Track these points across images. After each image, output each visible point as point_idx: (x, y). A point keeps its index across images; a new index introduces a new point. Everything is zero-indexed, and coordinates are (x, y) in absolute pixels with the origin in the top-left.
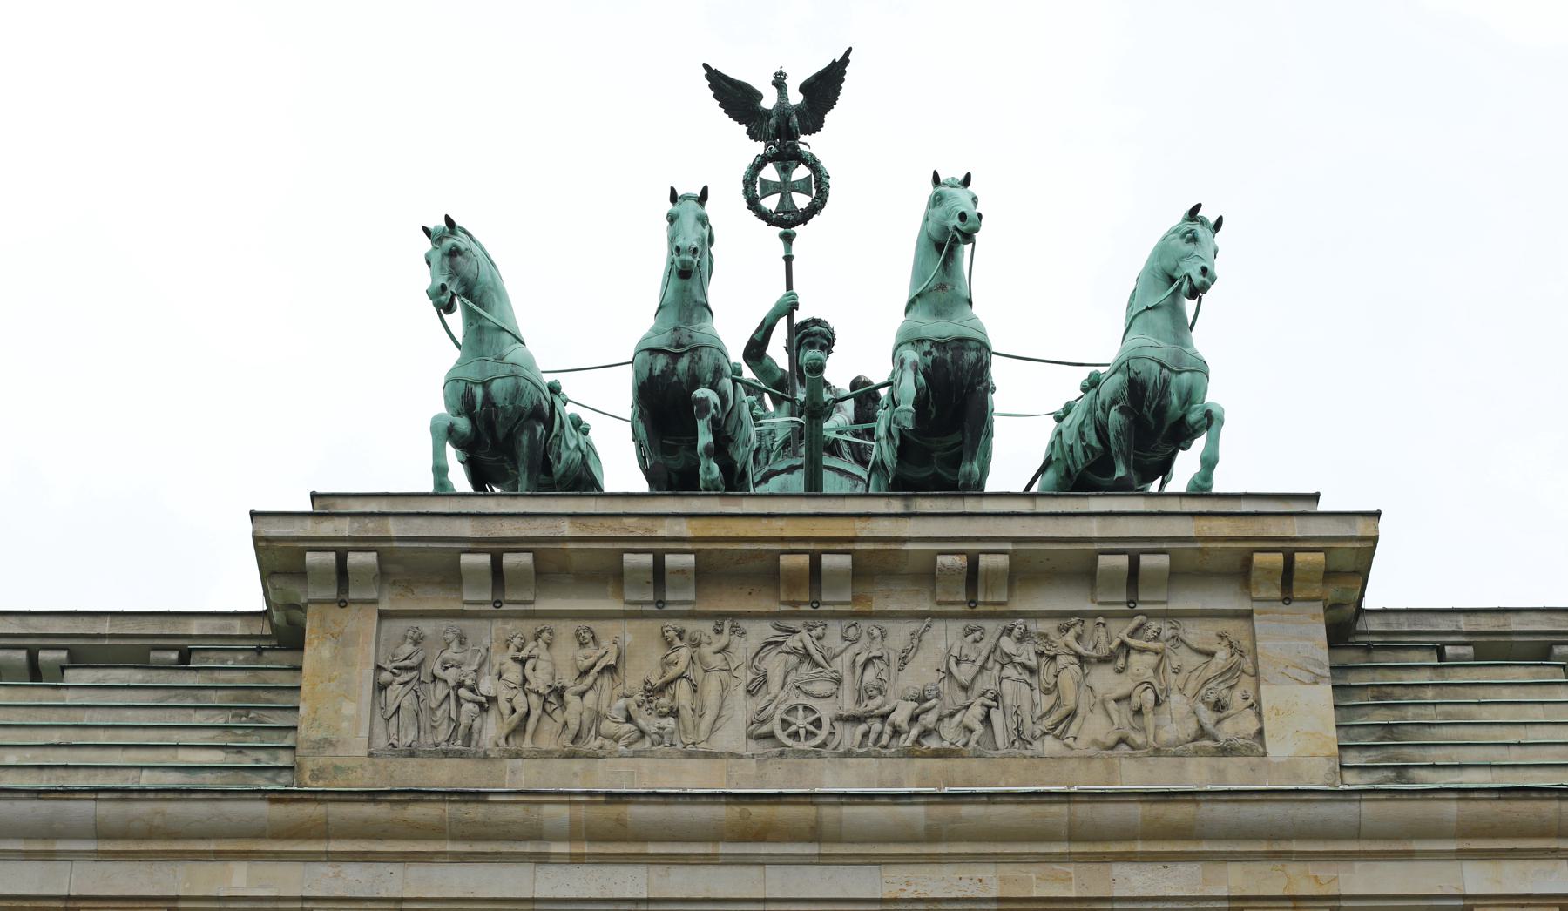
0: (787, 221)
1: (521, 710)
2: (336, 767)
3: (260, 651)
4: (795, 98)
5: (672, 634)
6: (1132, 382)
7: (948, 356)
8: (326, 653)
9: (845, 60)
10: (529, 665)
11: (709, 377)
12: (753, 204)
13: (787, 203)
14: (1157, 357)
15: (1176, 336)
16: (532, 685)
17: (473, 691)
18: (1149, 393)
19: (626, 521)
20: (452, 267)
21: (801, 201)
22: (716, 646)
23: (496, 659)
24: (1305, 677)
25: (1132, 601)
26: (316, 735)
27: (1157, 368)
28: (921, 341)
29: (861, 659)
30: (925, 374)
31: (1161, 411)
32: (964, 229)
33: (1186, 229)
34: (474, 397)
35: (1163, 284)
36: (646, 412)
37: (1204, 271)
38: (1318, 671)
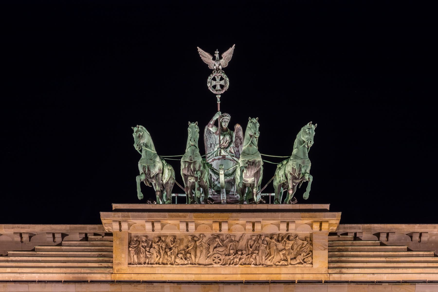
1: (159, 257)
2: (121, 269)
3: (103, 237)
5: (190, 239)
8: (118, 243)
10: (160, 245)
11: (198, 168)
16: (161, 251)
17: (149, 252)
22: (200, 241)
23: (153, 244)
24: (323, 249)
25: (288, 230)
26: (117, 262)
29: (229, 244)
34: (145, 169)
38: (326, 247)
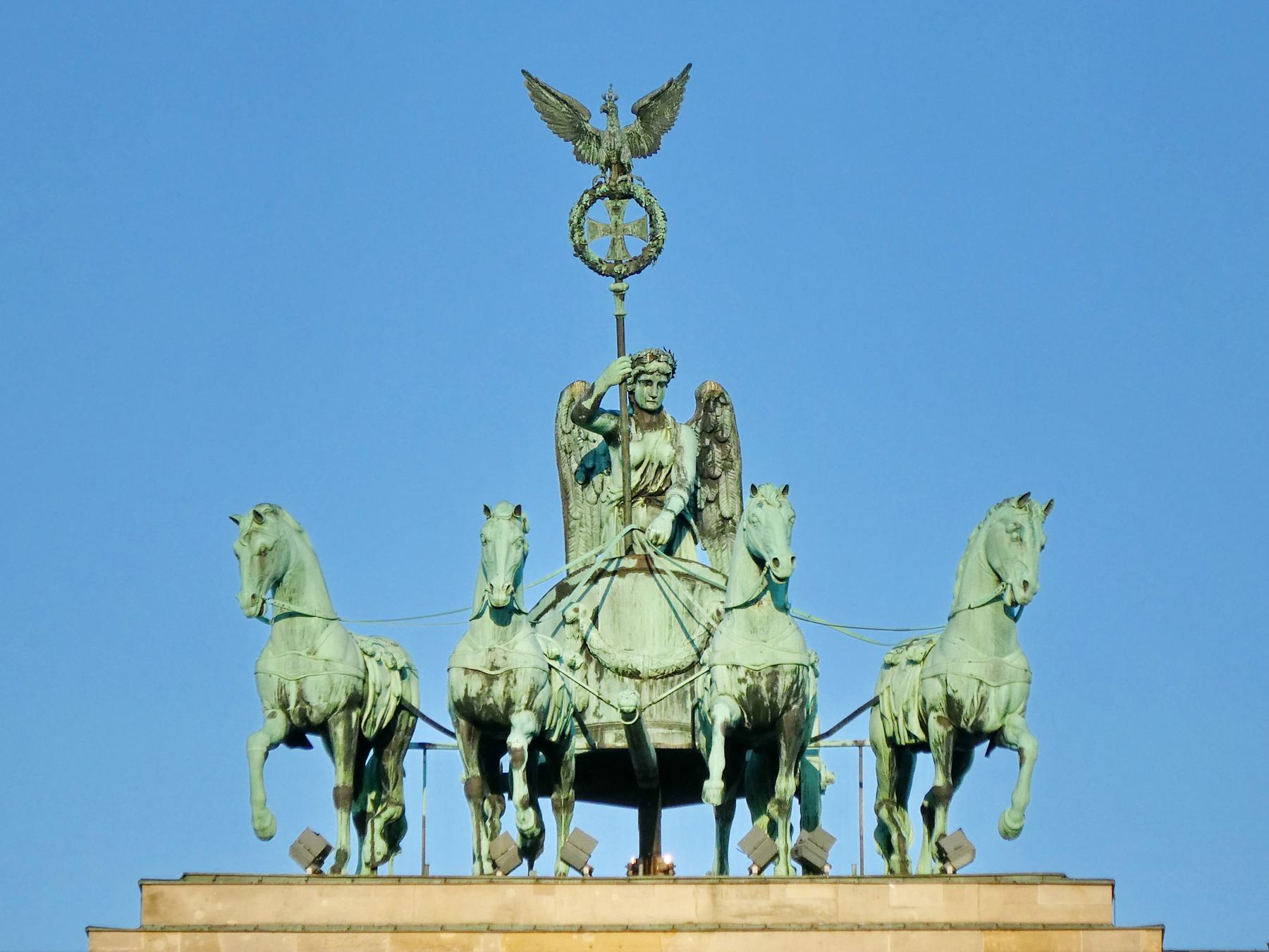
0: (619, 272)
4: (629, 121)
6: (949, 699)
7: (763, 684)
9: (684, 76)
11: (524, 700)
12: (580, 251)
13: (619, 247)
14: (975, 673)
15: (997, 643)
18: (966, 710)
19: (444, 936)
20: (263, 567)
21: (636, 247)
27: (976, 683)
28: (737, 666)
30: (739, 700)
31: (978, 725)
32: (780, 575)
33: (1012, 526)
34: (287, 696)
35: (993, 577)
36: (462, 722)
37: (1026, 584)
